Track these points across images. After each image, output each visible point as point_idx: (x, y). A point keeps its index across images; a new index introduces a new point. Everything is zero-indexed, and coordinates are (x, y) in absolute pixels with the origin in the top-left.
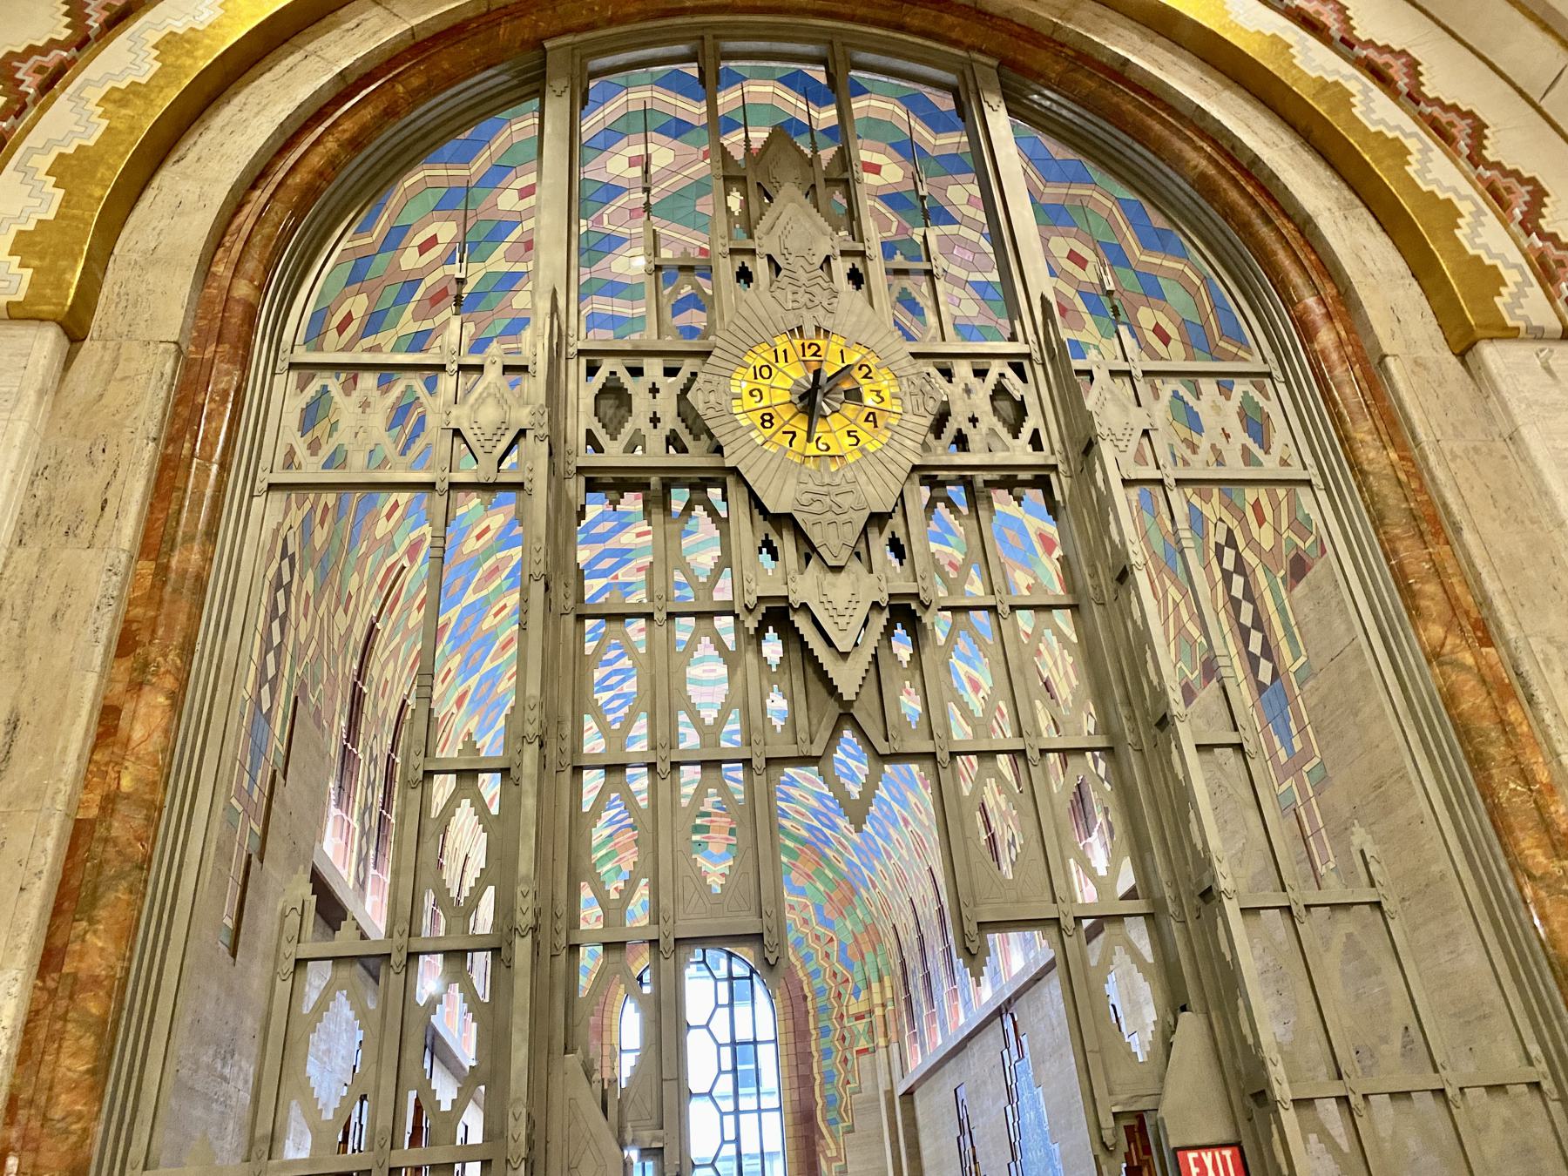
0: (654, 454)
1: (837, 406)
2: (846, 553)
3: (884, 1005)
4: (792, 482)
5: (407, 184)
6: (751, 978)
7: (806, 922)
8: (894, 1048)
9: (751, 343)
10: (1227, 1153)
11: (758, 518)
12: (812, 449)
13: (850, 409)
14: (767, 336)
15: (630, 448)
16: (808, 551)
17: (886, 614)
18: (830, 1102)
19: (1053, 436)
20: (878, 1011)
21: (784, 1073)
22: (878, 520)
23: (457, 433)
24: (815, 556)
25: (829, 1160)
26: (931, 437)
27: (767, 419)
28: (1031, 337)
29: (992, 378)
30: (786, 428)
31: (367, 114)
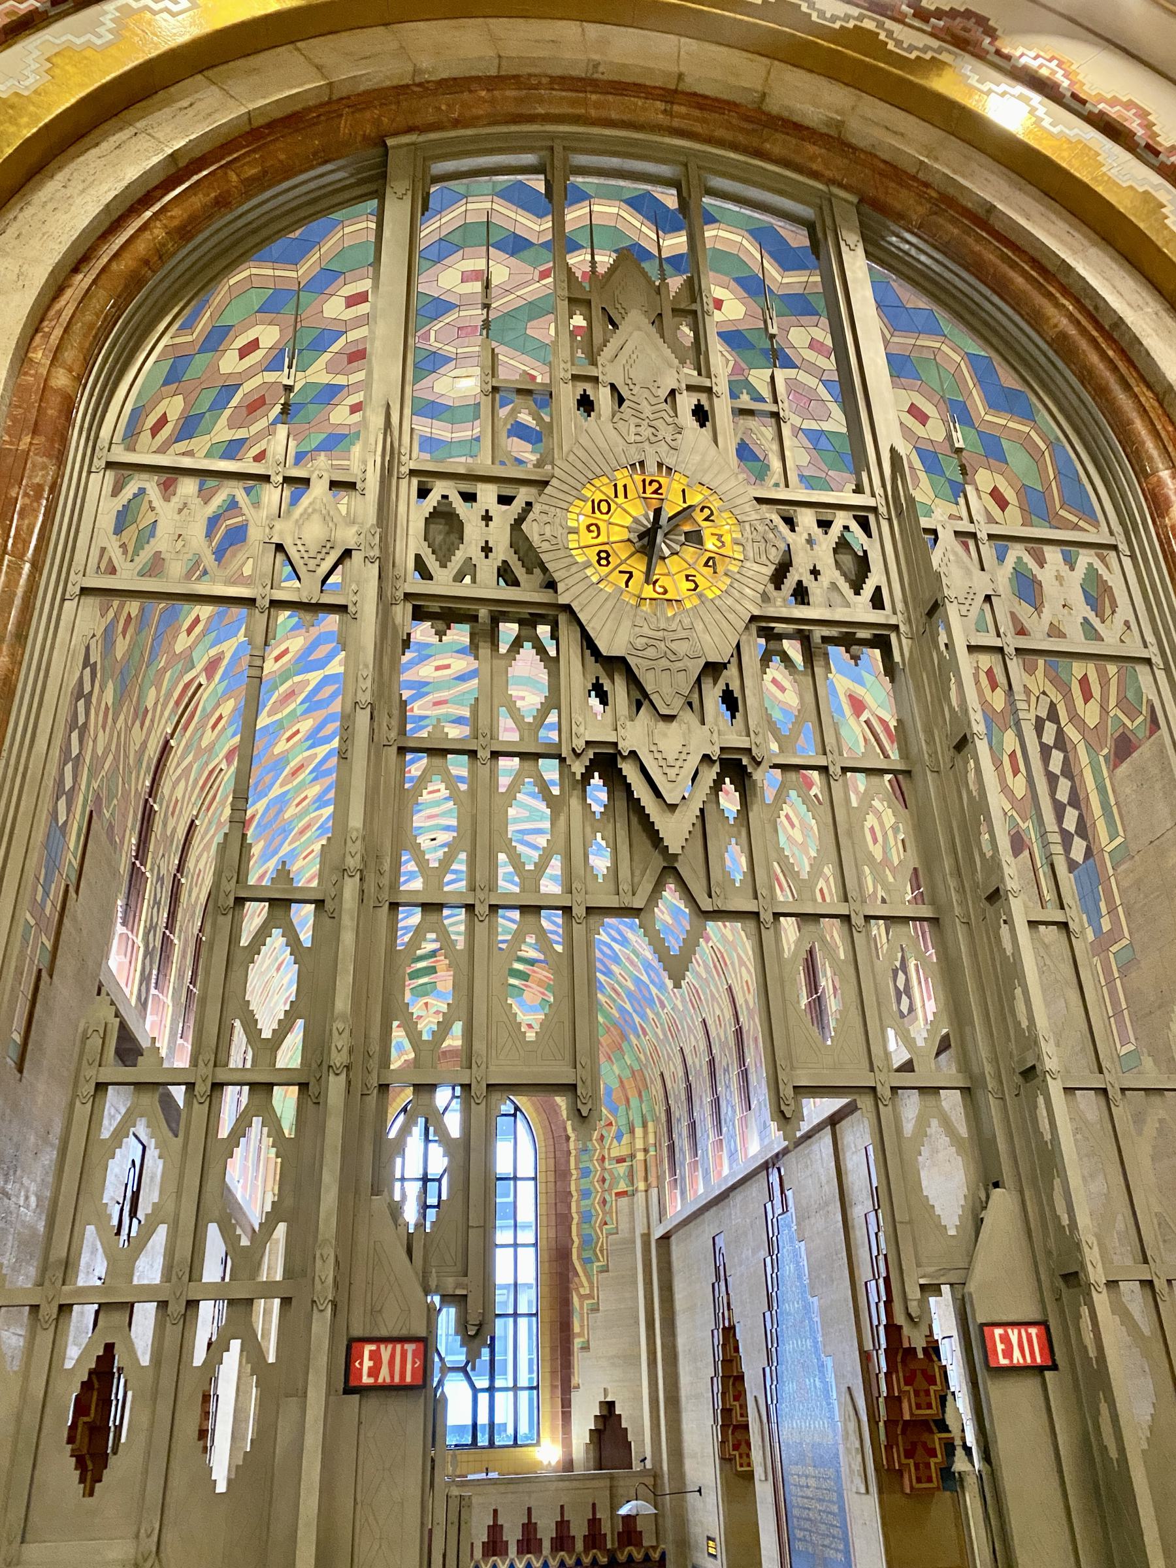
0: (486, 585)
1: (677, 548)
2: (679, 702)
3: (646, 1151)
4: (626, 624)
5: (232, 282)
6: (514, 1115)
8: (654, 1192)
9: (591, 476)
10: (1033, 1331)
11: (591, 660)
12: (648, 592)
13: (689, 552)
14: (607, 469)
15: (459, 577)
16: (641, 698)
17: (716, 768)
18: (587, 1242)
19: (894, 595)
20: (640, 1156)
21: (542, 1210)
22: (713, 669)
23: (280, 548)
24: (646, 703)
25: (581, 1297)
26: (771, 587)
27: (604, 557)
28: (878, 490)
29: (836, 530)
30: (623, 568)
31: (197, 201)
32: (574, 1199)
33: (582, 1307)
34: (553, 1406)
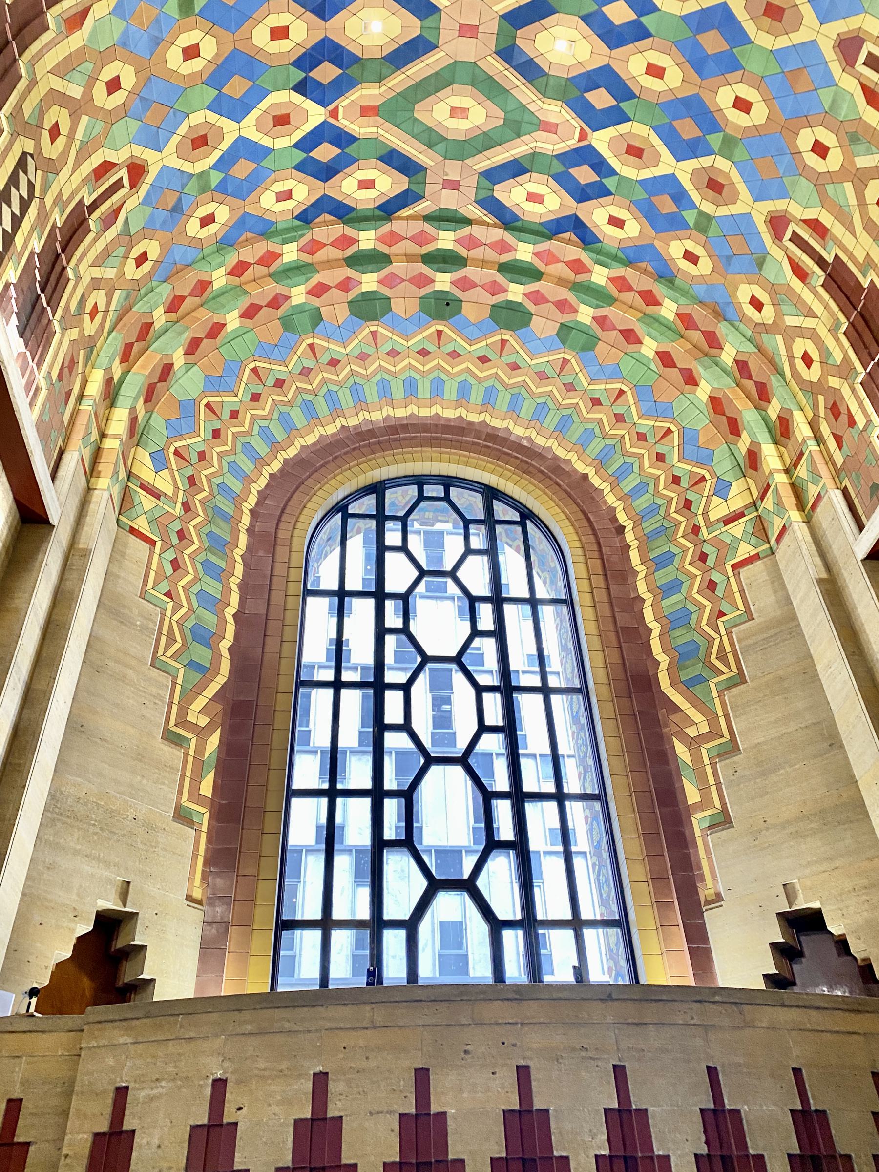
18: (682, 658)
25: (693, 743)
32: (648, 603)
33: (697, 758)
34: (666, 939)
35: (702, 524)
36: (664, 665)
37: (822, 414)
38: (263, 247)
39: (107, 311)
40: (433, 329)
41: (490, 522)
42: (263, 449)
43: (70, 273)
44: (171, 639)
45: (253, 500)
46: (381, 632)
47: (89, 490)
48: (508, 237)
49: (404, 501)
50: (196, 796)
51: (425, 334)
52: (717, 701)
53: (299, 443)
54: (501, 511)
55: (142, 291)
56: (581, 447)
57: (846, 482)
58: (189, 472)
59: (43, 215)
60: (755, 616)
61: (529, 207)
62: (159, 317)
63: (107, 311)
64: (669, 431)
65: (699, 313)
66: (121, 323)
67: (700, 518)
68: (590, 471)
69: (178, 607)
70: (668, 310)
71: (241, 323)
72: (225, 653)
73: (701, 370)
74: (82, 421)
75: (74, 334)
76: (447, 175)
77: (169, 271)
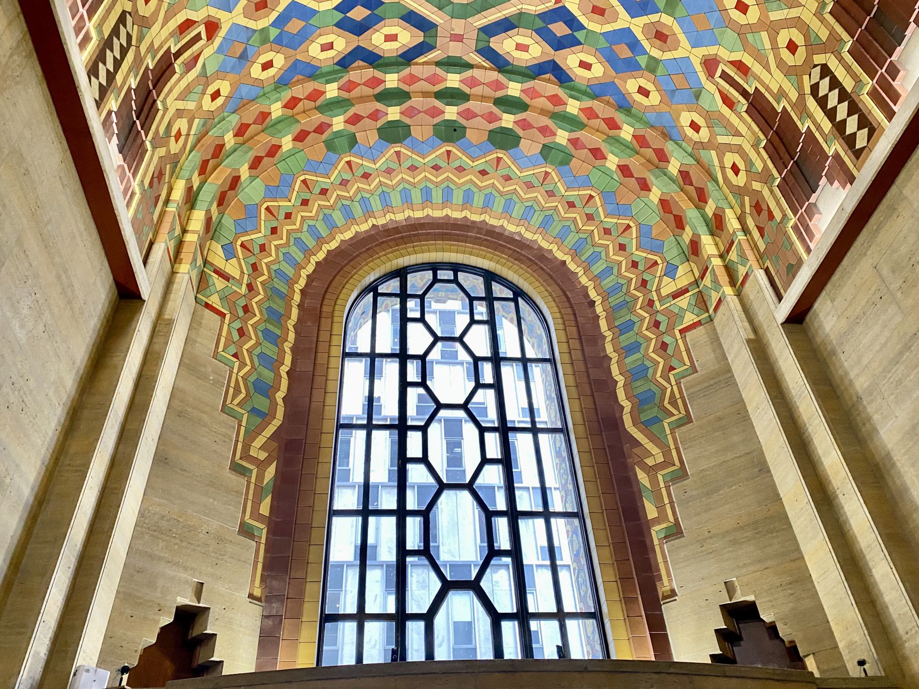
7: (590, 217)
18: (641, 402)
25: (651, 471)
32: (614, 361)
33: (654, 482)
35: (655, 298)
36: (627, 410)
37: (748, 211)
38: (311, 86)
39: (188, 135)
40: (443, 149)
41: (490, 299)
42: (311, 243)
43: (159, 104)
44: (237, 391)
45: (302, 282)
46: (404, 384)
47: (173, 273)
48: (501, 78)
49: (422, 283)
50: (256, 515)
51: (438, 153)
52: (669, 437)
53: (340, 237)
54: (498, 290)
55: (216, 120)
56: (560, 239)
57: (768, 263)
58: (252, 260)
59: (138, 60)
60: (698, 369)
61: (518, 54)
62: (229, 140)
63: (188, 135)
64: (628, 227)
65: (651, 135)
66: (199, 145)
67: (654, 294)
68: (568, 259)
69: (243, 365)
70: (627, 133)
71: (293, 144)
72: (280, 402)
73: (653, 178)
74: (168, 220)
75: (162, 152)
76: (453, 30)
77: (238, 104)
